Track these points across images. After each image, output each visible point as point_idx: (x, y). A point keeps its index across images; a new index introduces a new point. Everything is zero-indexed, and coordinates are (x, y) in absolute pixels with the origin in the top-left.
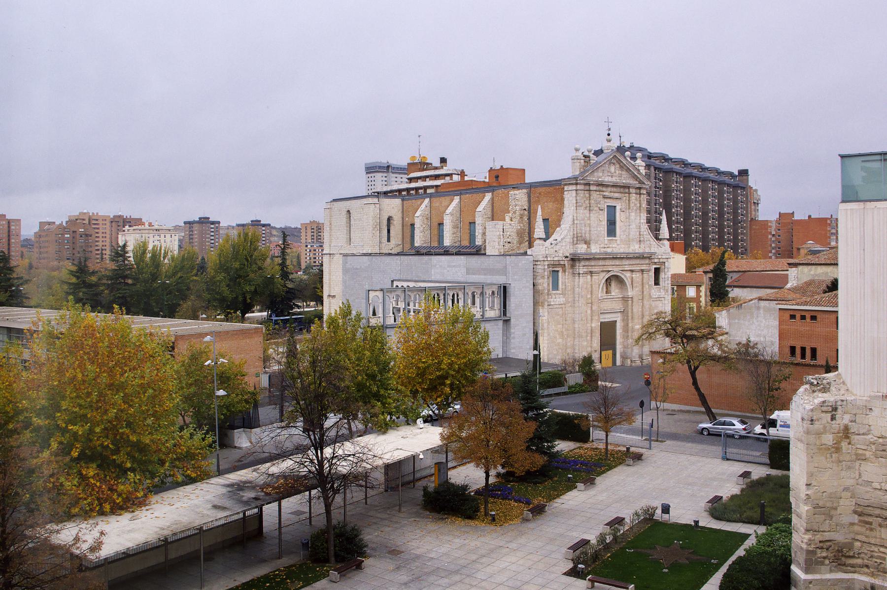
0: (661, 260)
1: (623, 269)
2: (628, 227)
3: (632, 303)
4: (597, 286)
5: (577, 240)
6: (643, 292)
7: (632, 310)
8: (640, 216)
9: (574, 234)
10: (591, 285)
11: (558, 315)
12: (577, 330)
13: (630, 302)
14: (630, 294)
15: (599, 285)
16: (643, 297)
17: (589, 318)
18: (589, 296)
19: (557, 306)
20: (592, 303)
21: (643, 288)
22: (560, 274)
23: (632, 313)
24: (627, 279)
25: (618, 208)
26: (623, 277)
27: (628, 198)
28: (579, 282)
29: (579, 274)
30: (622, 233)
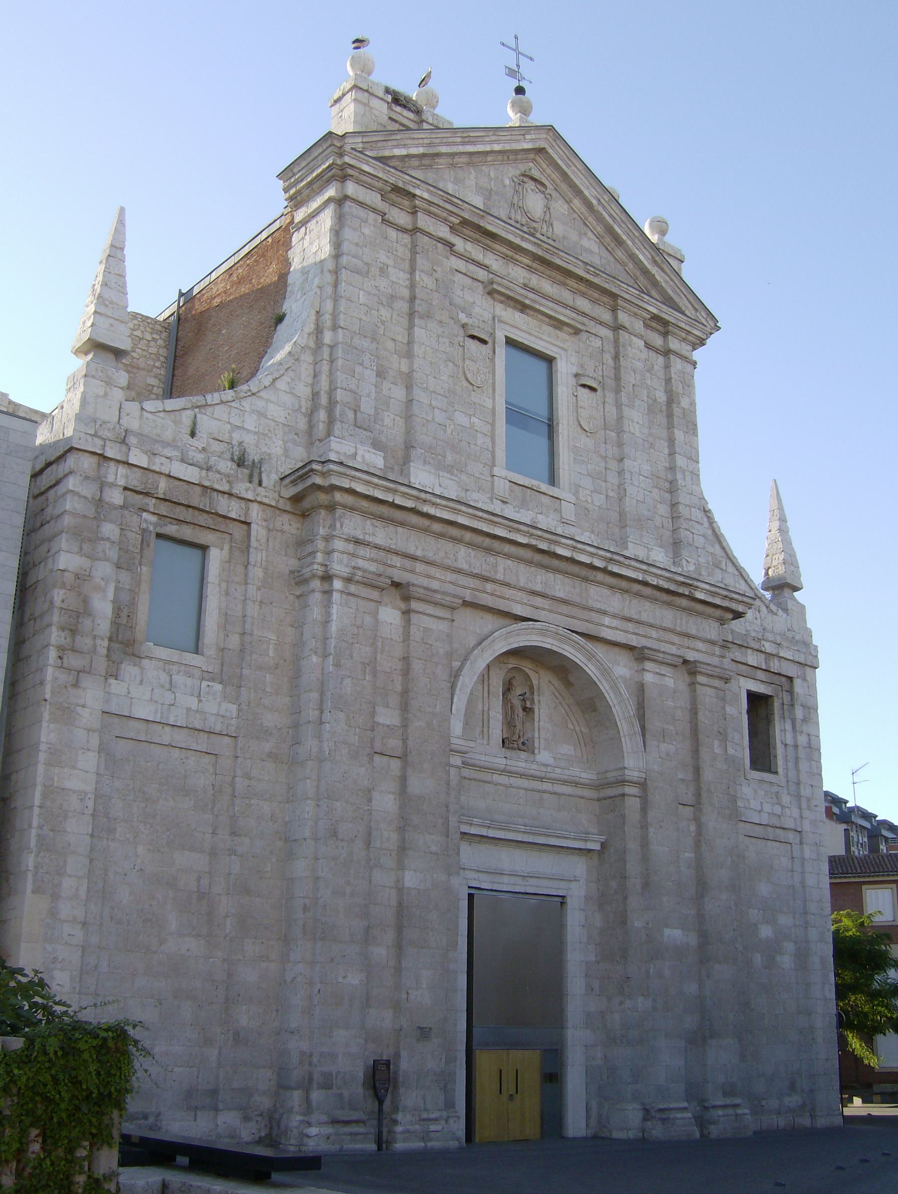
0: (775, 666)
1: (592, 630)
2: (613, 465)
3: (644, 810)
5: (331, 421)
6: (697, 771)
7: (645, 843)
8: (671, 441)
9: (315, 395)
10: (406, 659)
15: (455, 676)
16: (698, 794)
17: (388, 837)
18: (388, 717)
19: (180, 738)
20: (404, 757)
21: (696, 752)
22: (216, 556)
24: (615, 688)
25: (564, 369)
26: (591, 670)
28: (326, 622)
29: (327, 578)
30: (587, 482)
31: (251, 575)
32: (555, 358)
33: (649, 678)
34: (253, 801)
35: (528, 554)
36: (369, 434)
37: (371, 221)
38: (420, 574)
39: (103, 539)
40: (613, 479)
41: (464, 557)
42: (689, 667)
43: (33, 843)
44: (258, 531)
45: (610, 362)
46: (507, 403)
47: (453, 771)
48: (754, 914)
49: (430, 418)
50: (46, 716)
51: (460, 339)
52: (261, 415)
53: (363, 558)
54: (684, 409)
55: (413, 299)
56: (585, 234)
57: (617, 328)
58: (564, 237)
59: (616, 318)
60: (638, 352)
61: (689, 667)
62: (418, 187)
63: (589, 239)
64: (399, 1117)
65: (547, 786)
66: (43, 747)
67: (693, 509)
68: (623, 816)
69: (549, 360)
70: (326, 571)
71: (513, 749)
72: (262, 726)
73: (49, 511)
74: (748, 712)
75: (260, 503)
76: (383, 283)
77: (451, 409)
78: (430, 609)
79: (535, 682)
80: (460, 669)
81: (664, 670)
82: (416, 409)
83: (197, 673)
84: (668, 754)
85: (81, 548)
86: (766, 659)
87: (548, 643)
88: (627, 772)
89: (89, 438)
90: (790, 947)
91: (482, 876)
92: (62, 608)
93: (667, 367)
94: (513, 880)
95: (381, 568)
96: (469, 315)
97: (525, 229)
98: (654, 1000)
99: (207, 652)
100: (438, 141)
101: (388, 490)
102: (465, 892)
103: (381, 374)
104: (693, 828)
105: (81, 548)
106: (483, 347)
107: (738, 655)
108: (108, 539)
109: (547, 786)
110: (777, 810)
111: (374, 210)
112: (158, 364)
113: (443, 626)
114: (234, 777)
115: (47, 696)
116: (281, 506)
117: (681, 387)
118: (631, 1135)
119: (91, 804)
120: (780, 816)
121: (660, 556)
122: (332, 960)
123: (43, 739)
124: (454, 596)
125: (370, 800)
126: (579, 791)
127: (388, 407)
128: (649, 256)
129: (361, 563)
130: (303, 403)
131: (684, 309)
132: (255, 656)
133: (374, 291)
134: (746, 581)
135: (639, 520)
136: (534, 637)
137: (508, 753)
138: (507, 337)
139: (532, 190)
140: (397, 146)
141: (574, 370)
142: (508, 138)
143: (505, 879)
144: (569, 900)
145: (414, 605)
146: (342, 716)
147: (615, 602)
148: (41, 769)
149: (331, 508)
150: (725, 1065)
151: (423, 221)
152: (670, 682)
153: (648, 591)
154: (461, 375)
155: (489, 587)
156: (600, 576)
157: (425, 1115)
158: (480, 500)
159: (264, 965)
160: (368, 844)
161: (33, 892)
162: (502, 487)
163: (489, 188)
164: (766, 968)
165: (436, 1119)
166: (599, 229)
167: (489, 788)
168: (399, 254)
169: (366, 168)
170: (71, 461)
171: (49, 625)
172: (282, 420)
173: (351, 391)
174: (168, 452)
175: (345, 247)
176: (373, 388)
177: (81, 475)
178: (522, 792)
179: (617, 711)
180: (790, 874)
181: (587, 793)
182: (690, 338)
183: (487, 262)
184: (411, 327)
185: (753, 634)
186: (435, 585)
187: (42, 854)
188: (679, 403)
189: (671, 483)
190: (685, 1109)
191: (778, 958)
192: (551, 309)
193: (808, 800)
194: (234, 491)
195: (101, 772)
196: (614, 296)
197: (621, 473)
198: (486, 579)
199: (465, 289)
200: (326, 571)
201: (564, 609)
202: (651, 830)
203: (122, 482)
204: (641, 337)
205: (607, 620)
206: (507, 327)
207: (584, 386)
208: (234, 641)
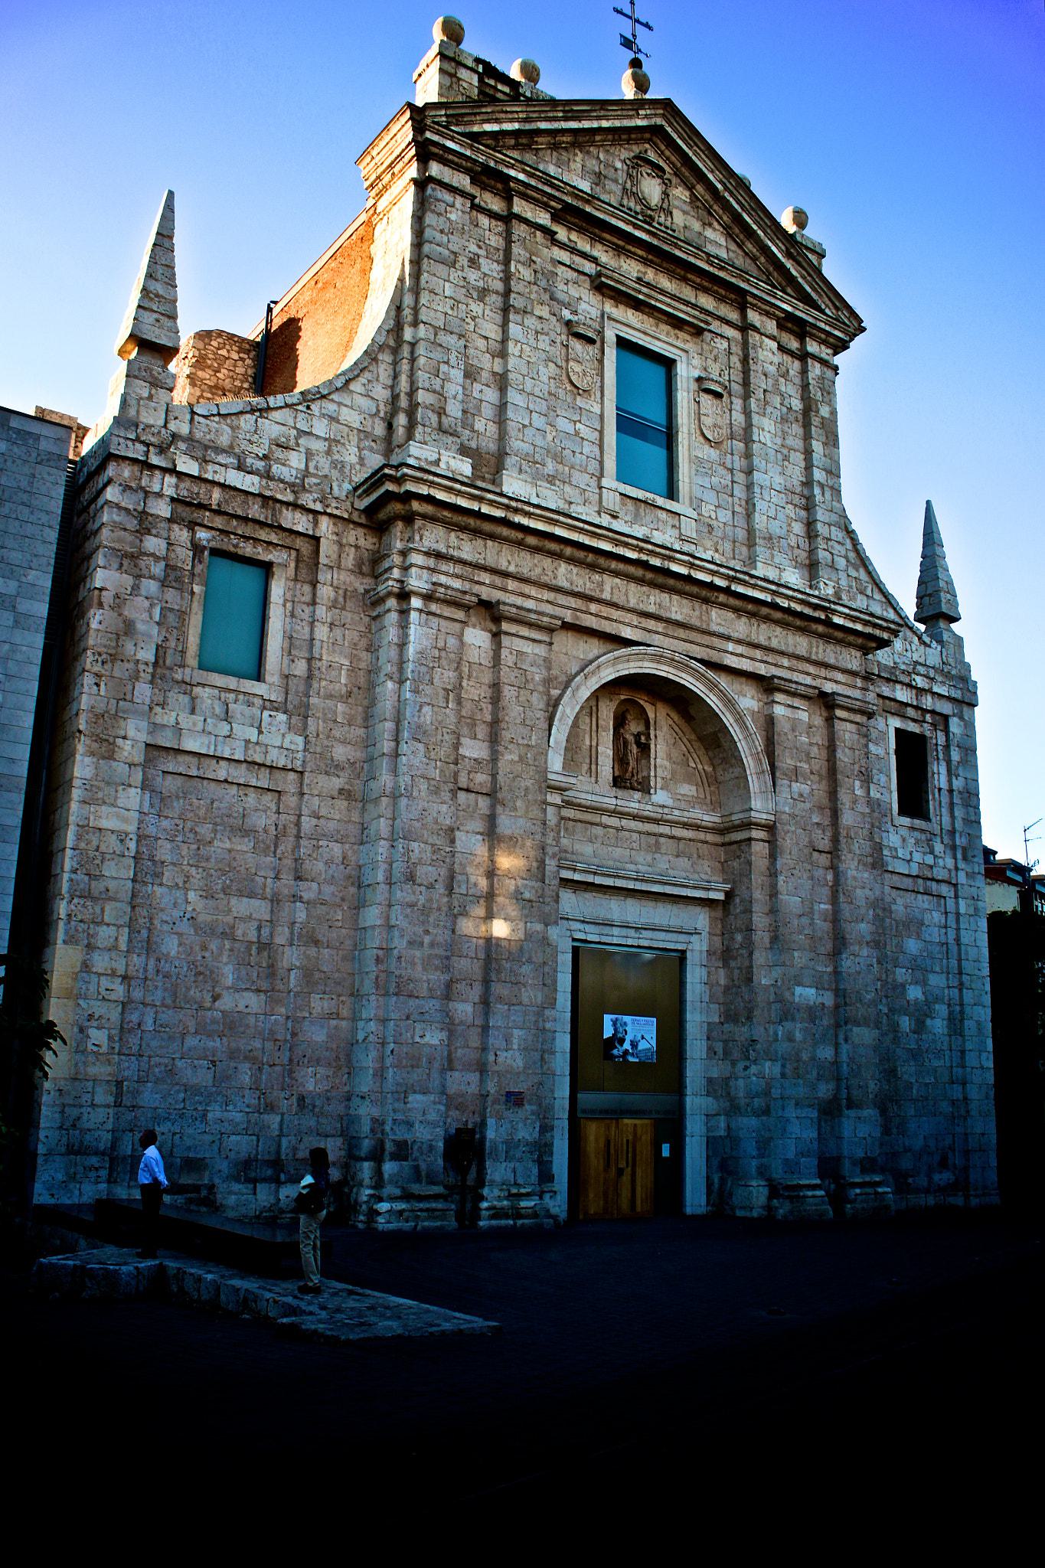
0: (928, 702)
1: (715, 656)
2: (740, 477)
3: (773, 856)
4: (538, 701)
6: (835, 814)
7: (774, 893)
9: (395, 397)
10: (496, 687)
11: (245, 832)
12: (375, 940)
13: (759, 849)
14: (760, 807)
15: (553, 705)
16: (835, 840)
18: (474, 749)
19: (240, 774)
20: (492, 794)
21: (833, 794)
23: (773, 911)
24: (740, 720)
25: (686, 372)
26: (713, 701)
27: (737, 349)
28: (402, 645)
29: (404, 596)
30: (710, 497)
31: (319, 593)
32: (674, 361)
33: (779, 710)
34: (321, 843)
35: (639, 572)
36: (455, 439)
37: (458, 205)
38: (513, 592)
39: (145, 554)
40: (739, 492)
41: (565, 574)
42: (826, 702)
43: (65, 887)
44: (327, 549)
45: (738, 365)
46: (618, 409)
47: (550, 809)
48: (901, 974)
49: (526, 422)
50: (80, 748)
51: (564, 337)
52: (333, 419)
53: (446, 574)
54: (823, 418)
55: (507, 293)
56: (710, 225)
57: (745, 328)
58: (685, 227)
59: (744, 316)
60: (770, 355)
61: (826, 702)
62: (512, 167)
63: (715, 229)
64: (486, 1192)
65: (665, 830)
66: (76, 783)
67: (833, 528)
68: (750, 863)
69: (669, 364)
70: (402, 588)
71: (625, 788)
72: (332, 760)
73: (90, 527)
74: (897, 752)
75: (330, 515)
76: (473, 276)
77: (552, 413)
78: (525, 631)
79: (651, 715)
80: (561, 696)
81: (797, 702)
82: (510, 414)
83: (258, 702)
84: (801, 795)
85: (121, 565)
86: (917, 695)
87: (664, 671)
88: (753, 814)
89: (130, 444)
90: (942, 1009)
91: (588, 928)
92: (98, 630)
93: (804, 372)
94: (624, 932)
95: (467, 586)
96: (575, 313)
97: (640, 217)
98: (783, 1066)
99: (268, 678)
100: (535, 115)
101: (473, 497)
102: (566, 946)
103: (470, 374)
104: (830, 877)
105: (121, 565)
106: (590, 348)
107: (886, 690)
108: (153, 555)
109: (665, 830)
110: (929, 859)
111: (463, 193)
112: (246, 385)
113: (541, 650)
114: (300, 816)
115: (81, 727)
116: (356, 519)
117: (820, 394)
118: (755, 1214)
119: (132, 845)
120: (931, 867)
121: (793, 578)
122: (408, 1018)
123: (76, 774)
124: (552, 617)
125: (453, 841)
126: (701, 836)
127: (480, 411)
128: (783, 248)
129: (443, 579)
130: (382, 407)
131: (823, 307)
132: (323, 683)
133: (462, 283)
134: (895, 609)
135: (771, 538)
136: (646, 664)
137: (620, 793)
138: (618, 336)
139: (648, 174)
140: (488, 121)
141: (696, 374)
142: (619, 113)
143: (616, 931)
144: (689, 955)
145: (505, 626)
146: (421, 746)
147: (741, 627)
148: (74, 806)
149: (409, 519)
150: (865, 1139)
151: (519, 206)
152: (804, 716)
153: (778, 615)
154: (564, 377)
155: (594, 607)
156: (722, 598)
157: (514, 1191)
158: (588, 513)
159: (333, 1023)
160: (450, 889)
161: (65, 942)
162: (611, 500)
163: (597, 170)
164: (915, 1033)
165: (528, 1195)
166: (725, 218)
167: (599, 831)
168: (492, 243)
169: (450, 144)
170: (111, 470)
171: (85, 650)
172: (357, 425)
173: (434, 392)
174: (221, 459)
175: (428, 233)
176: (460, 388)
177: (120, 485)
178: (635, 836)
179: (742, 746)
180: (944, 931)
181: (710, 837)
182: (831, 340)
183: (595, 253)
184: (504, 325)
185: (903, 667)
186: (530, 604)
187: (76, 900)
188: (817, 411)
189: (808, 499)
190: (814, 1187)
191: (928, 1022)
192: (669, 305)
193: (964, 849)
194: (300, 502)
195: (146, 811)
196: (743, 293)
197: (749, 487)
198: (591, 599)
199: (570, 284)
200: (402, 588)
201: (681, 633)
202: (781, 879)
203: (170, 491)
204: (773, 338)
205: (731, 647)
206: (619, 326)
207: (708, 391)
208: (300, 668)
